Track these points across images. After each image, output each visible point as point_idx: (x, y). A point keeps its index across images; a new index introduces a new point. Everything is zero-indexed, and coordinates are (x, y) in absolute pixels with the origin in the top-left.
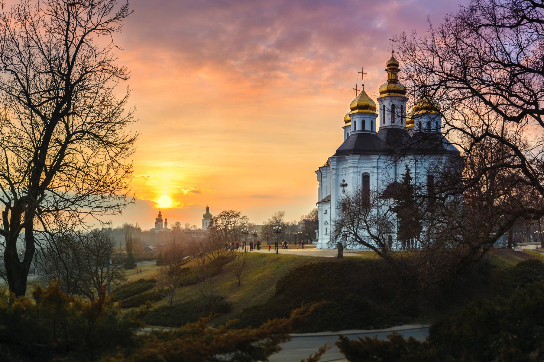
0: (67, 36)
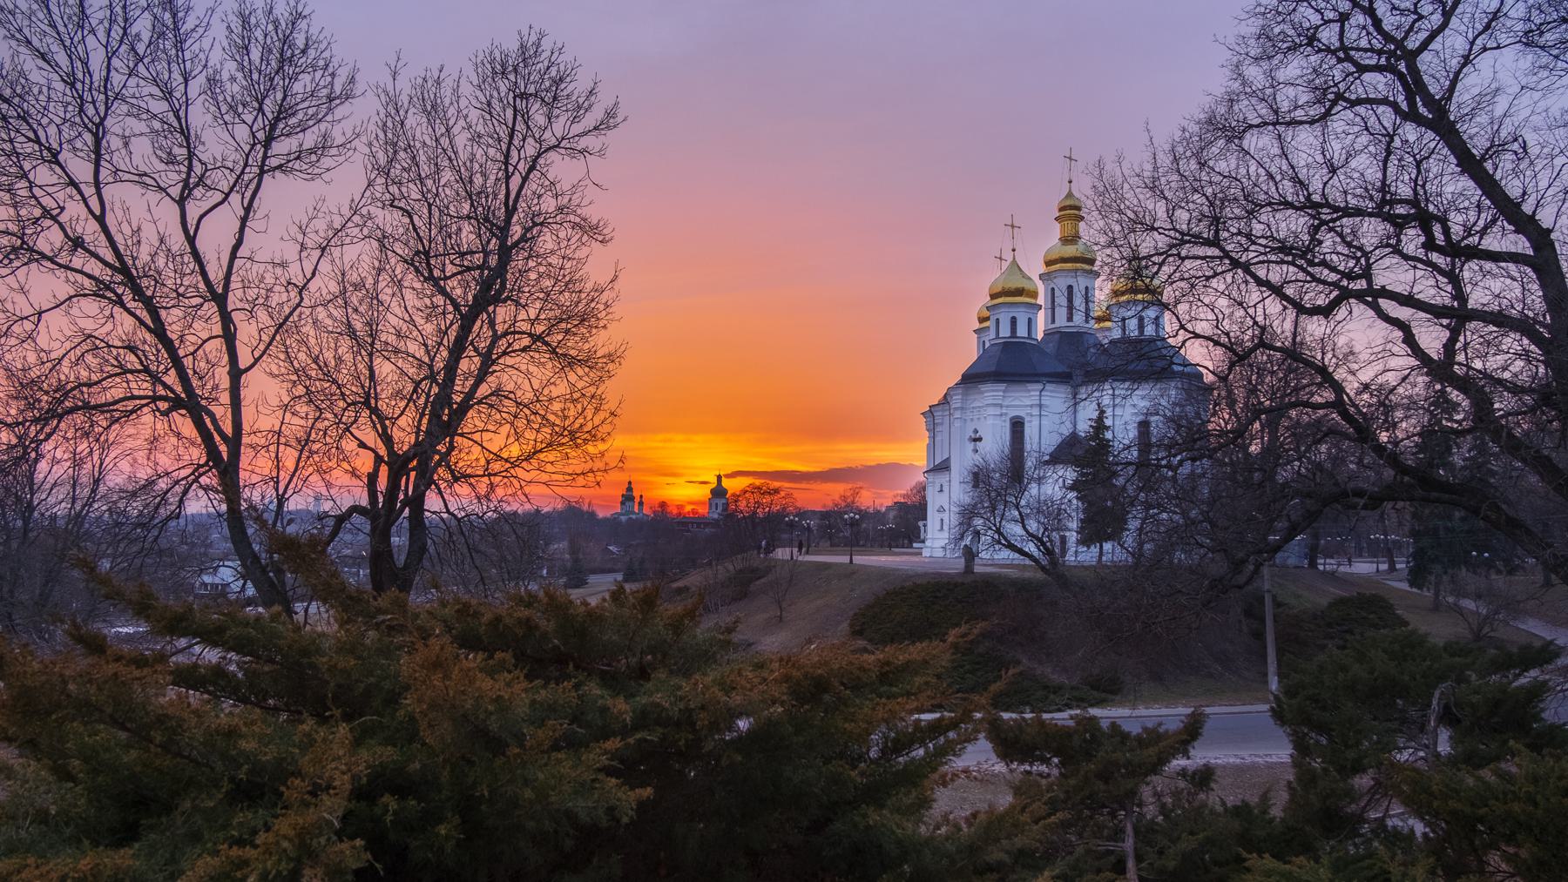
0: (507, 156)
